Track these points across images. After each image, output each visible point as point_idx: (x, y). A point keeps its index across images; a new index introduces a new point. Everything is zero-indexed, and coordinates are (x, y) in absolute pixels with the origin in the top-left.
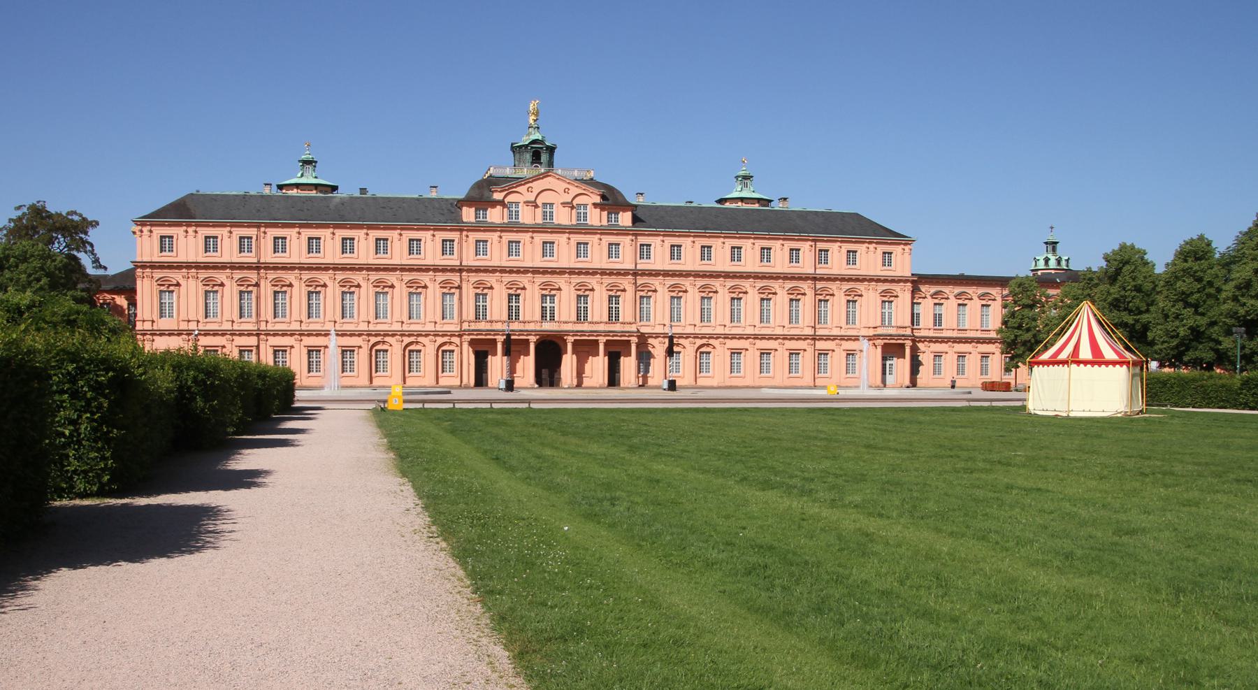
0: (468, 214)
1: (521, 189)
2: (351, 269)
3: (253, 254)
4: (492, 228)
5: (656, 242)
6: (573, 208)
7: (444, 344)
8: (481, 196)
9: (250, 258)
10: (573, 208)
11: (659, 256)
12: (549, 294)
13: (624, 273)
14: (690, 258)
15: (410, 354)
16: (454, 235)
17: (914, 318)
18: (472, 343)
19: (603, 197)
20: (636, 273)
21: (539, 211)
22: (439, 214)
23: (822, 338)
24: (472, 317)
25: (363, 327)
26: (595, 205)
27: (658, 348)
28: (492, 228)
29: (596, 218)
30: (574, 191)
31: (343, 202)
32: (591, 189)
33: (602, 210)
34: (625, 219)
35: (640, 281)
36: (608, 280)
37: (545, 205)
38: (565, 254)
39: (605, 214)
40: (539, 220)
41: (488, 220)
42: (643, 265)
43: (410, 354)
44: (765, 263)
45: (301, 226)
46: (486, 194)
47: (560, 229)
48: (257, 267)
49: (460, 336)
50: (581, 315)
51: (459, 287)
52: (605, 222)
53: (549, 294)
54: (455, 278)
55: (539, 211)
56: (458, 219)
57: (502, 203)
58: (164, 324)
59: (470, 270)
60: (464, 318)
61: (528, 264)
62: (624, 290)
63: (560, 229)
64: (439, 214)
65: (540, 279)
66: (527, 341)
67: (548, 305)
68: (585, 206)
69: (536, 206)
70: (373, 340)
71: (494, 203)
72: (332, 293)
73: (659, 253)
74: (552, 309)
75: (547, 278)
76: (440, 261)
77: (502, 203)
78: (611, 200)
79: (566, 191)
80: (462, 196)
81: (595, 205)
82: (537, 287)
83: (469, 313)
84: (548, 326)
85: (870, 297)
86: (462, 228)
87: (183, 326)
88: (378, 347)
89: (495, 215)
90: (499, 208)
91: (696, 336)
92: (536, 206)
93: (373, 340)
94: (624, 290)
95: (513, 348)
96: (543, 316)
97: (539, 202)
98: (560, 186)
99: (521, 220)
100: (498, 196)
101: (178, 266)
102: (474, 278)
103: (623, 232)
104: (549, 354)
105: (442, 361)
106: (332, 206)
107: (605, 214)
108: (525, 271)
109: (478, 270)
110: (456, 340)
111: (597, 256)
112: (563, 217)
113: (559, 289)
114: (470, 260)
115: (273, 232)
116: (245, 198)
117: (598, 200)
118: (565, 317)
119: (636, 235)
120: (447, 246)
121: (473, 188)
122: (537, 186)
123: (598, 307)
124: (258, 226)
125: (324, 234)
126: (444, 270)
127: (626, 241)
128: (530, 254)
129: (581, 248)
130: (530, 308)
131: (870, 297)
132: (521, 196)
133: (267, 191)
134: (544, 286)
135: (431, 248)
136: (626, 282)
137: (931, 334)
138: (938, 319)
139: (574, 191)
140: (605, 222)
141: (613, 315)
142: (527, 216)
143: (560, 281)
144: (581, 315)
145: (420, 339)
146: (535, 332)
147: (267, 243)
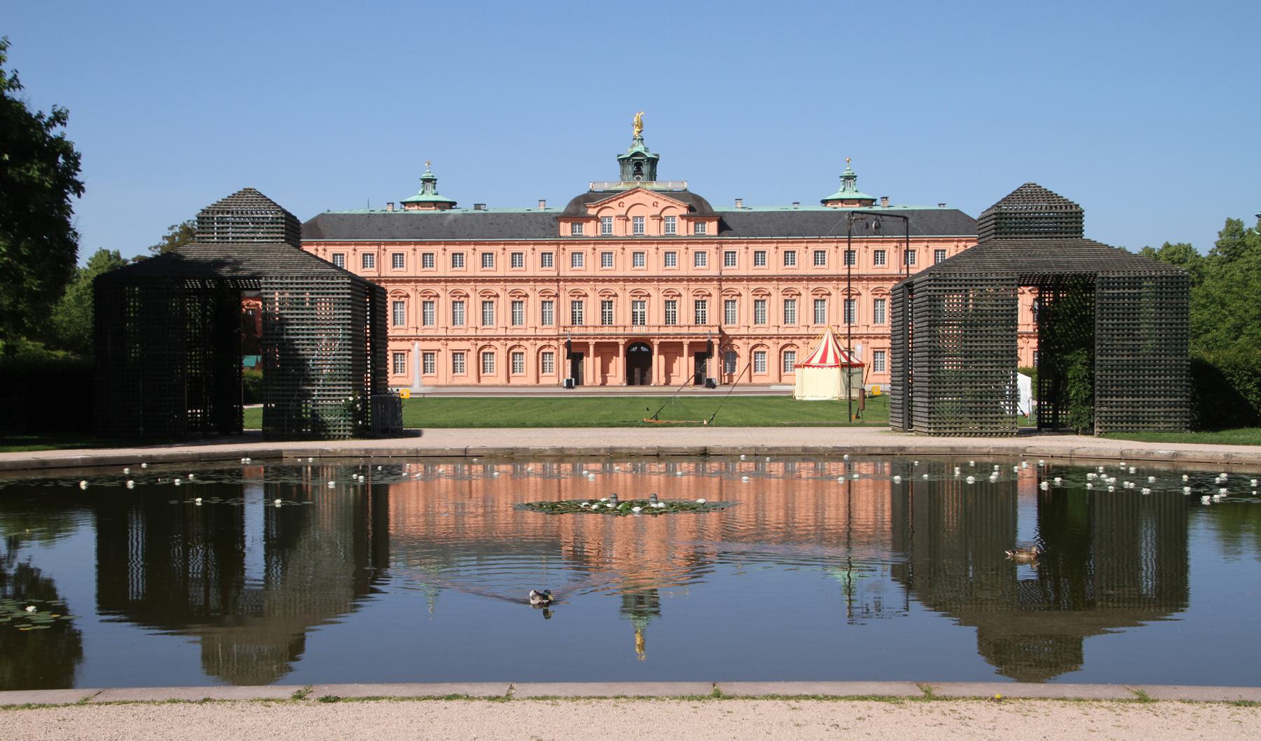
0: (565, 229)
2: (460, 281)
4: (586, 241)
5: (739, 249)
6: (661, 219)
7: (544, 347)
8: (577, 212)
10: (661, 219)
11: (744, 263)
12: (639, 300)
13: (711, 279)
14: (774, 263)
15: (513, 357)
16: (552, 249)
18: (568, 345)
19: (691, 209)
20: (720, 279)
21: (630, 224)
22: (536, 228)
24: (569, 322)
25: (472, 332)
26: (682, 217)
27: (742, 349)
28: (586, 241)
29: (683, 229)
30: (662, 204)
31: (456, 219)
32: (678, 202)
33: (689, 220)
34: (711, 228)
35: (725, 286)
36: (694, 286)
38: (653, 263)
39: (692, 224)
40: (630, 233)
41: (584, 234)
42: (728, 271)
43: (513, 357)
45: (416, 243)
46: (582, 210)
47: (649, 241)
49: (557, 340)
50: (670, 318)
51: (557, 296)
52: (692, 232)
53: (639, 300)
54: (553, 288)
55: (630, 224)
56: (556, 233)
57: (596, 218)
59: (566, 280)
60: (562, 323)
61: (619, 273)
62: (710, 295)
63: (649, 241)
64: (536, 228)
65: (631, 286)
67: (639, 310)
68: (673, 217)
69: (627, 220)
70: (481, 344)
71: (588, 219)
72: (443, 304)
73: (744, 263)
74: (643, 314)
75: (638, 286)
76: (540, 272)
77: (596, 218)
78: (697, 210)
80: (561, 209)
81: (682, 217)
82: (628, 295)
83: (566, 318)
84: (638, 330)
86: (560, 242)
88: (486, 350)
89: (589, 229)
90: (593, 223)
91: (779, 337)
92: (627, 220)
93: (481, 344)
94: (710, 295)
95: (606, 350)
96: (634, 321)
97: (630, 216)
99: (613, 233)
102: (570, 287)
103: (708, 241)
104: (638, 359)
105: (541, 367)
106: (445, 224)
107: (692, 224)
108: (616, 280)
109: (573, 280)
110: (554, 343)
111: (684, 264)
112: (651, 229)
113: (649, 295)
114: (567, 271)
115: (392, 249)
116: (369, 218)
117: (684, 211)
118: (654, 323)
119: (721, 243)
120: (545, 259)
121: (570, 204)
124: (379, 244)
125: (436, 250)
127: (711, 249)
128: (622, 264)
129: (669, 258)
130: (622, 313)
132: (613, 210)
133: (390, 210)
134: (635, 292)
135: (531, 263)
136: (712, 288)
140: (692, 232)
141: (700, 319)
142: (618, 229)
143: (649, 288)
144: (670, 318)
145: (522, 343)
146: (624, 336)
147: (387, 260)
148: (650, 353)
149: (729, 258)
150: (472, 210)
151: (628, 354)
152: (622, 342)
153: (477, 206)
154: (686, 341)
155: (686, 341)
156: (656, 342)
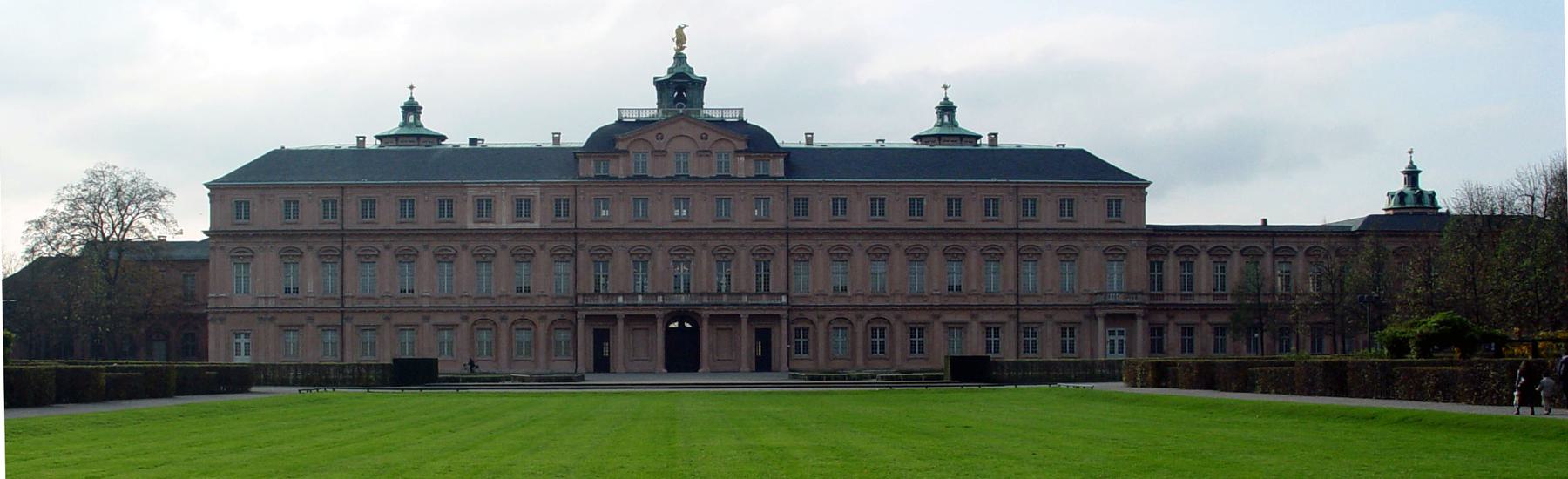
0: (588, 168)
1: (651, 136)
3: (338, 220)
9: (332, 225)
17: (1157, 282)
23: (1028, 308)
29: (743, 167)
34: (777, 167)
37: (678, 154)
38: (701, 213)
44: (954, 217)
48: (342, 235)
58: (242, 301)
66: (654, 317)
77: (626, 152)
79: (704, 137)
85: (1091, 255)
87: (262, 304)
89: (618, 168)
98: (696, 132)
100: (621, 146)
101: (257, 235)
109: (594, 234)
111: (744, 214)
112: (697, 168)
114: (586, 223)
117: (742, 146)
122: (668, 132)
123: (743, 275)
126: (557, 234)
131: (1091, 255)
136: (776, 243)
137: (1178, 300)
138: (1188, 283)
139: (713, 136)
148: (696, 331)
149: (801, 206)
150: (465, 144)
151: (668, 331)
152: (659, 313)
153: (473, 141)
154: (744, 315)
155: (744, 315)
156: (705, 313)
